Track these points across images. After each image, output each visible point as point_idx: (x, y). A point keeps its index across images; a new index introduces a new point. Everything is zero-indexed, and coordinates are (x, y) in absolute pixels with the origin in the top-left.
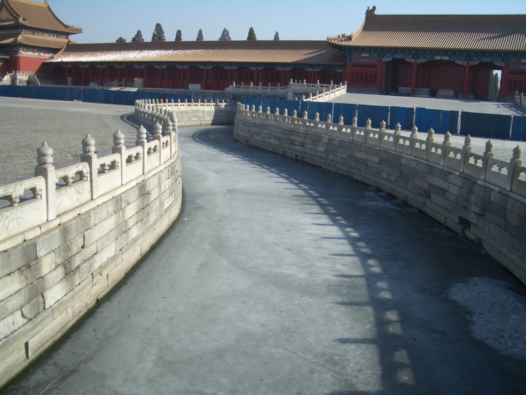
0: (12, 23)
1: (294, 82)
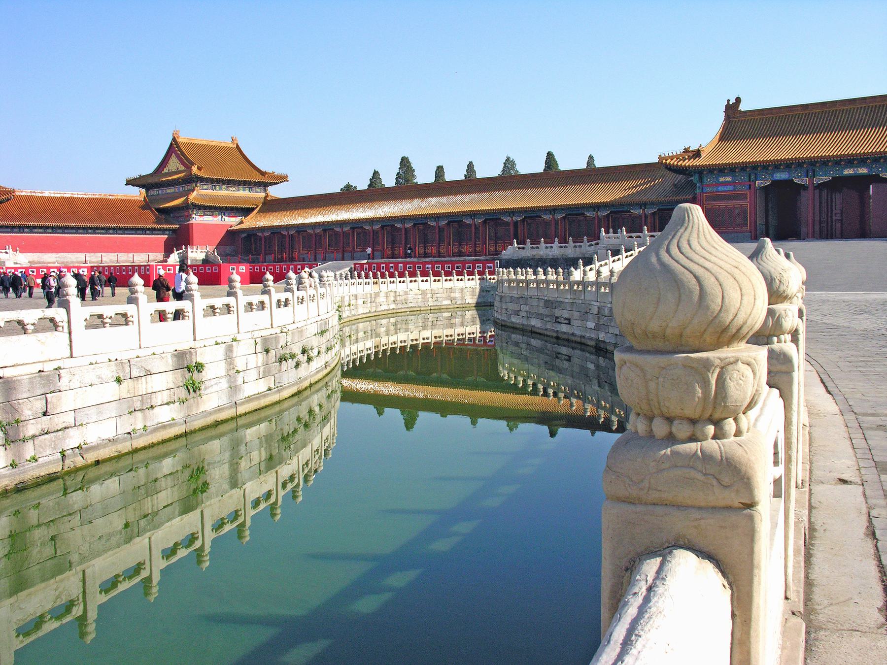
0: (182, 175)
1: (607, 232)
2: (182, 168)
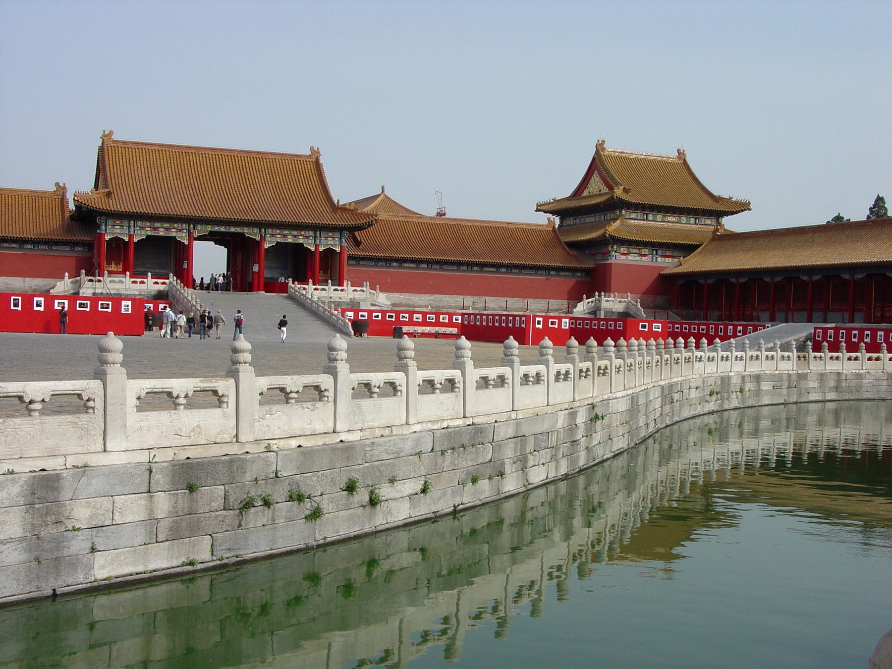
2: (605, 190)
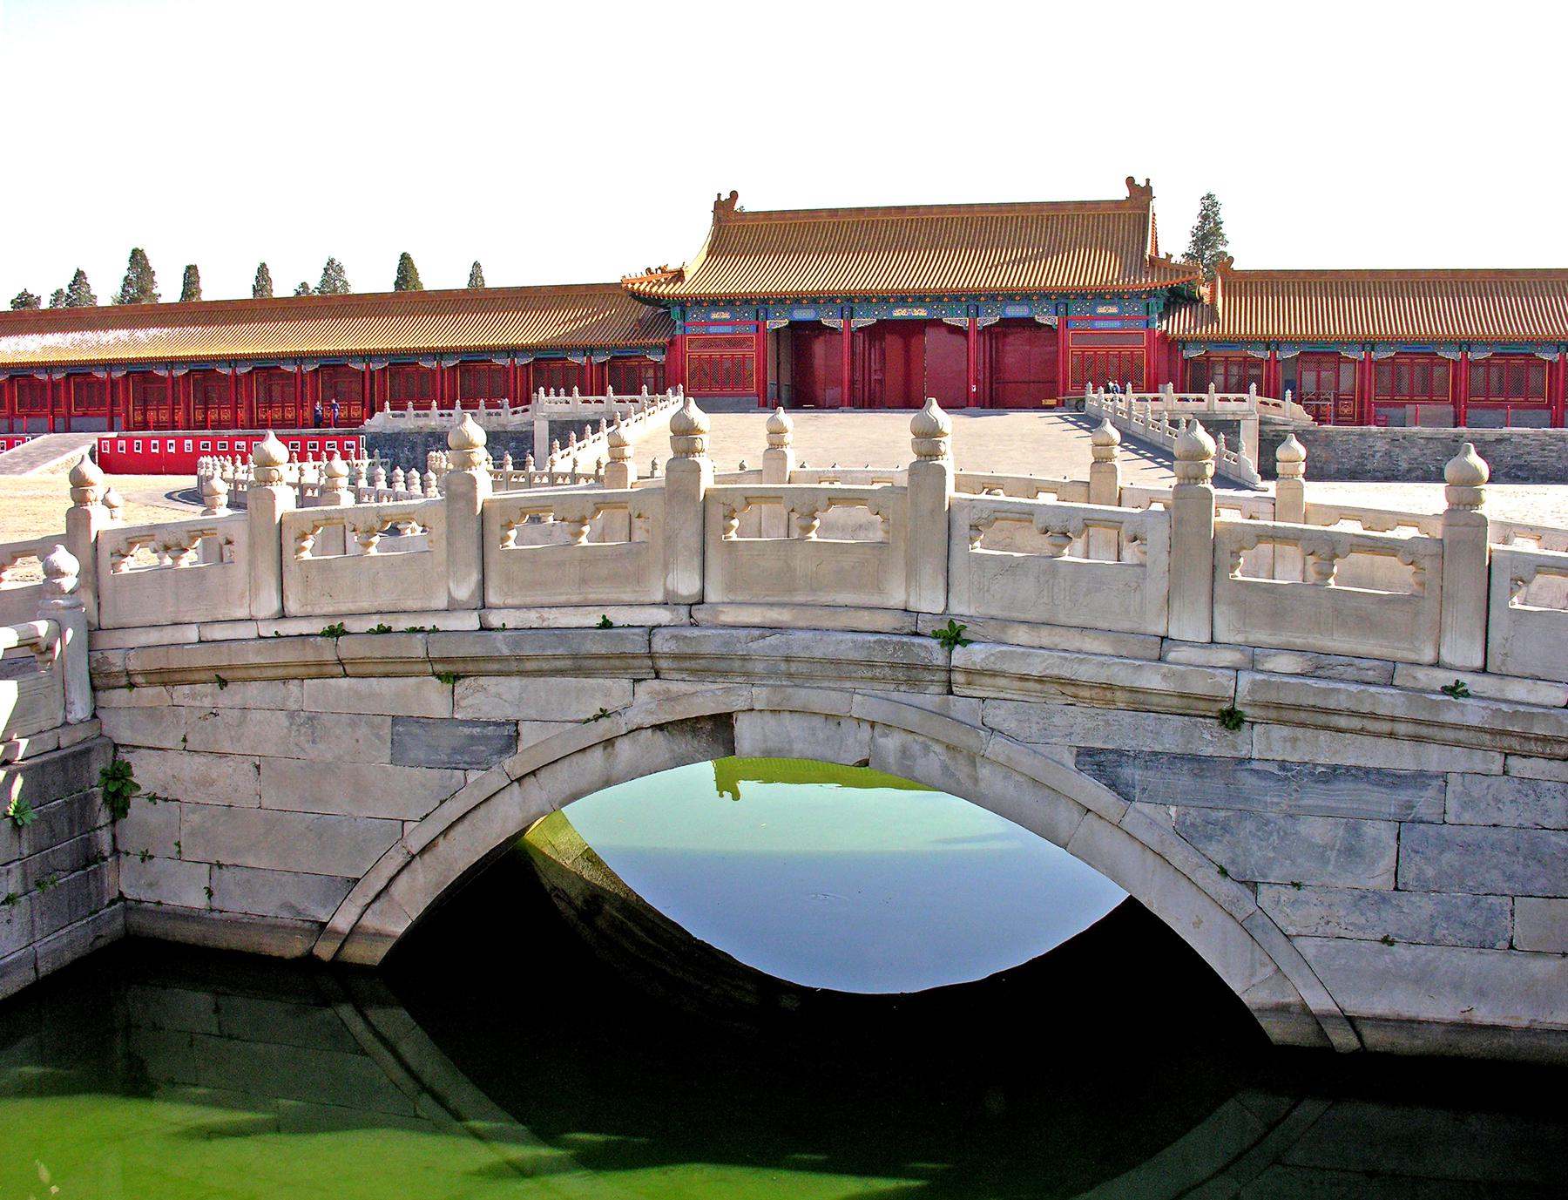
1: (547, 394)
